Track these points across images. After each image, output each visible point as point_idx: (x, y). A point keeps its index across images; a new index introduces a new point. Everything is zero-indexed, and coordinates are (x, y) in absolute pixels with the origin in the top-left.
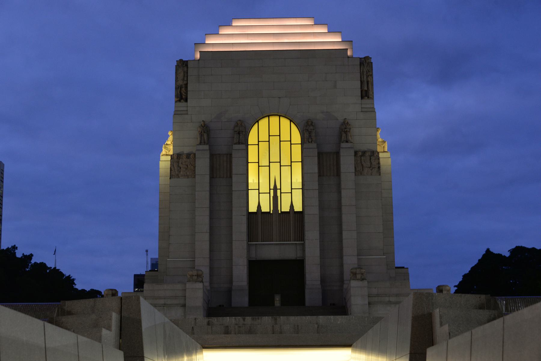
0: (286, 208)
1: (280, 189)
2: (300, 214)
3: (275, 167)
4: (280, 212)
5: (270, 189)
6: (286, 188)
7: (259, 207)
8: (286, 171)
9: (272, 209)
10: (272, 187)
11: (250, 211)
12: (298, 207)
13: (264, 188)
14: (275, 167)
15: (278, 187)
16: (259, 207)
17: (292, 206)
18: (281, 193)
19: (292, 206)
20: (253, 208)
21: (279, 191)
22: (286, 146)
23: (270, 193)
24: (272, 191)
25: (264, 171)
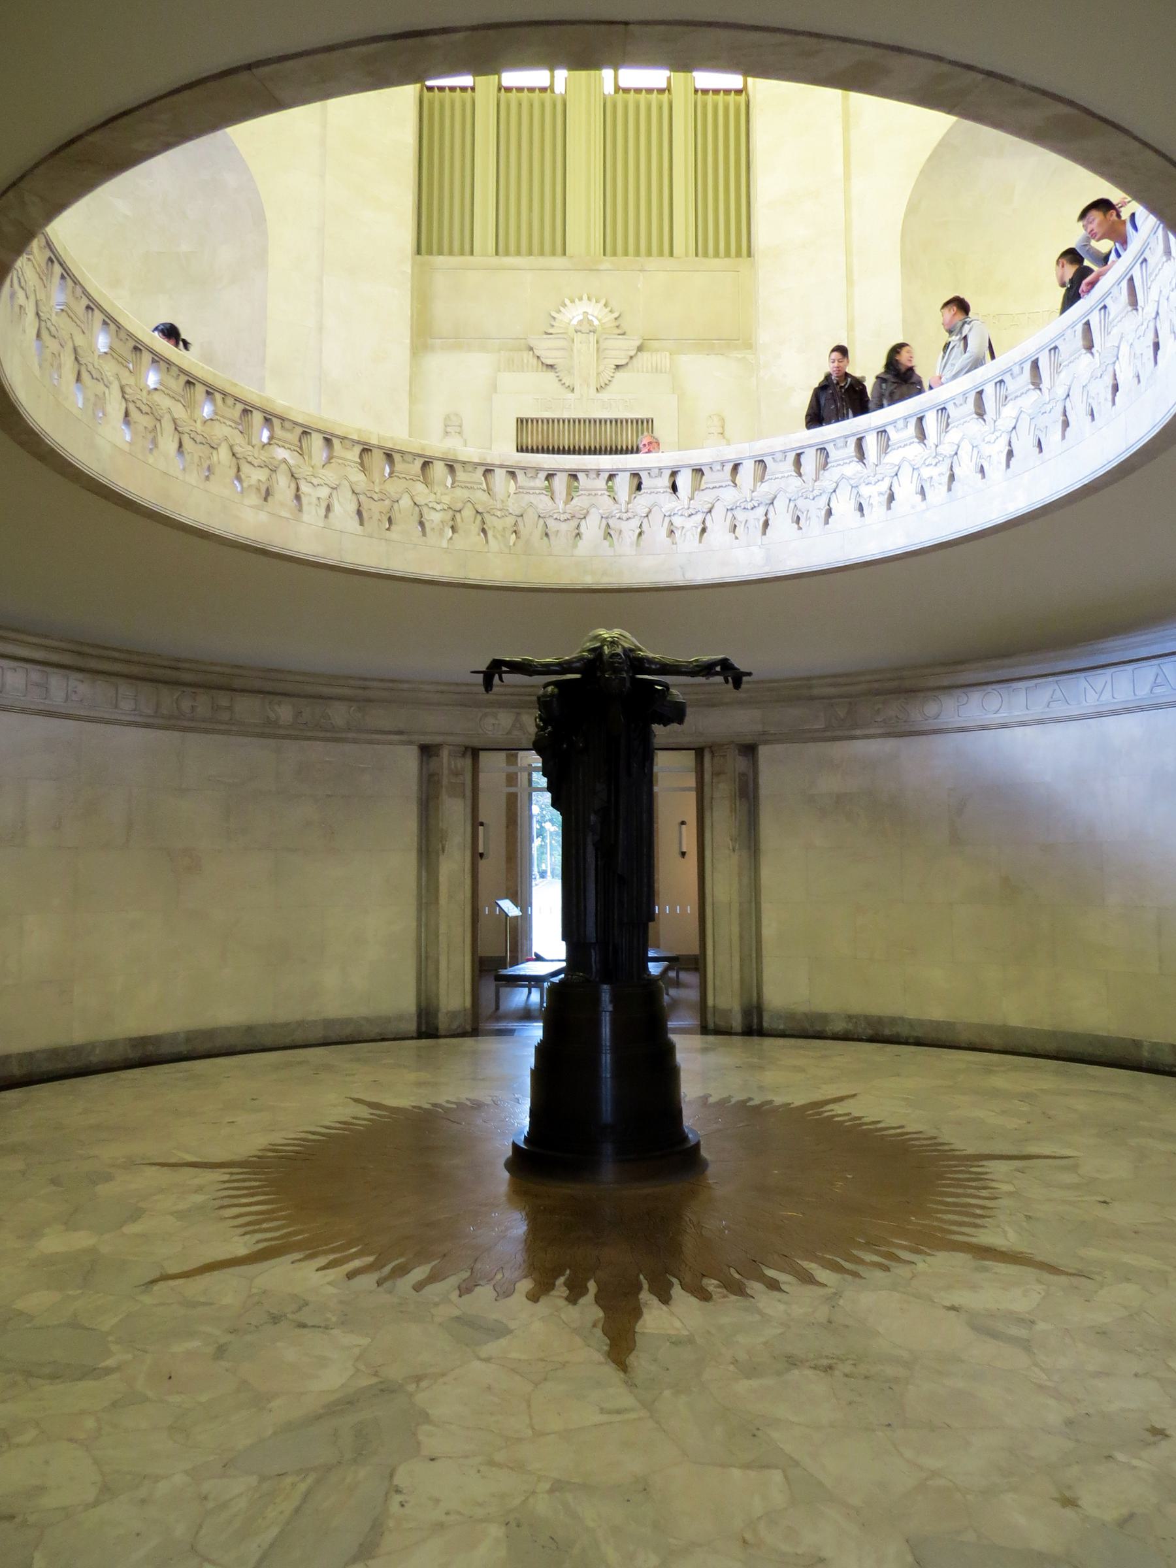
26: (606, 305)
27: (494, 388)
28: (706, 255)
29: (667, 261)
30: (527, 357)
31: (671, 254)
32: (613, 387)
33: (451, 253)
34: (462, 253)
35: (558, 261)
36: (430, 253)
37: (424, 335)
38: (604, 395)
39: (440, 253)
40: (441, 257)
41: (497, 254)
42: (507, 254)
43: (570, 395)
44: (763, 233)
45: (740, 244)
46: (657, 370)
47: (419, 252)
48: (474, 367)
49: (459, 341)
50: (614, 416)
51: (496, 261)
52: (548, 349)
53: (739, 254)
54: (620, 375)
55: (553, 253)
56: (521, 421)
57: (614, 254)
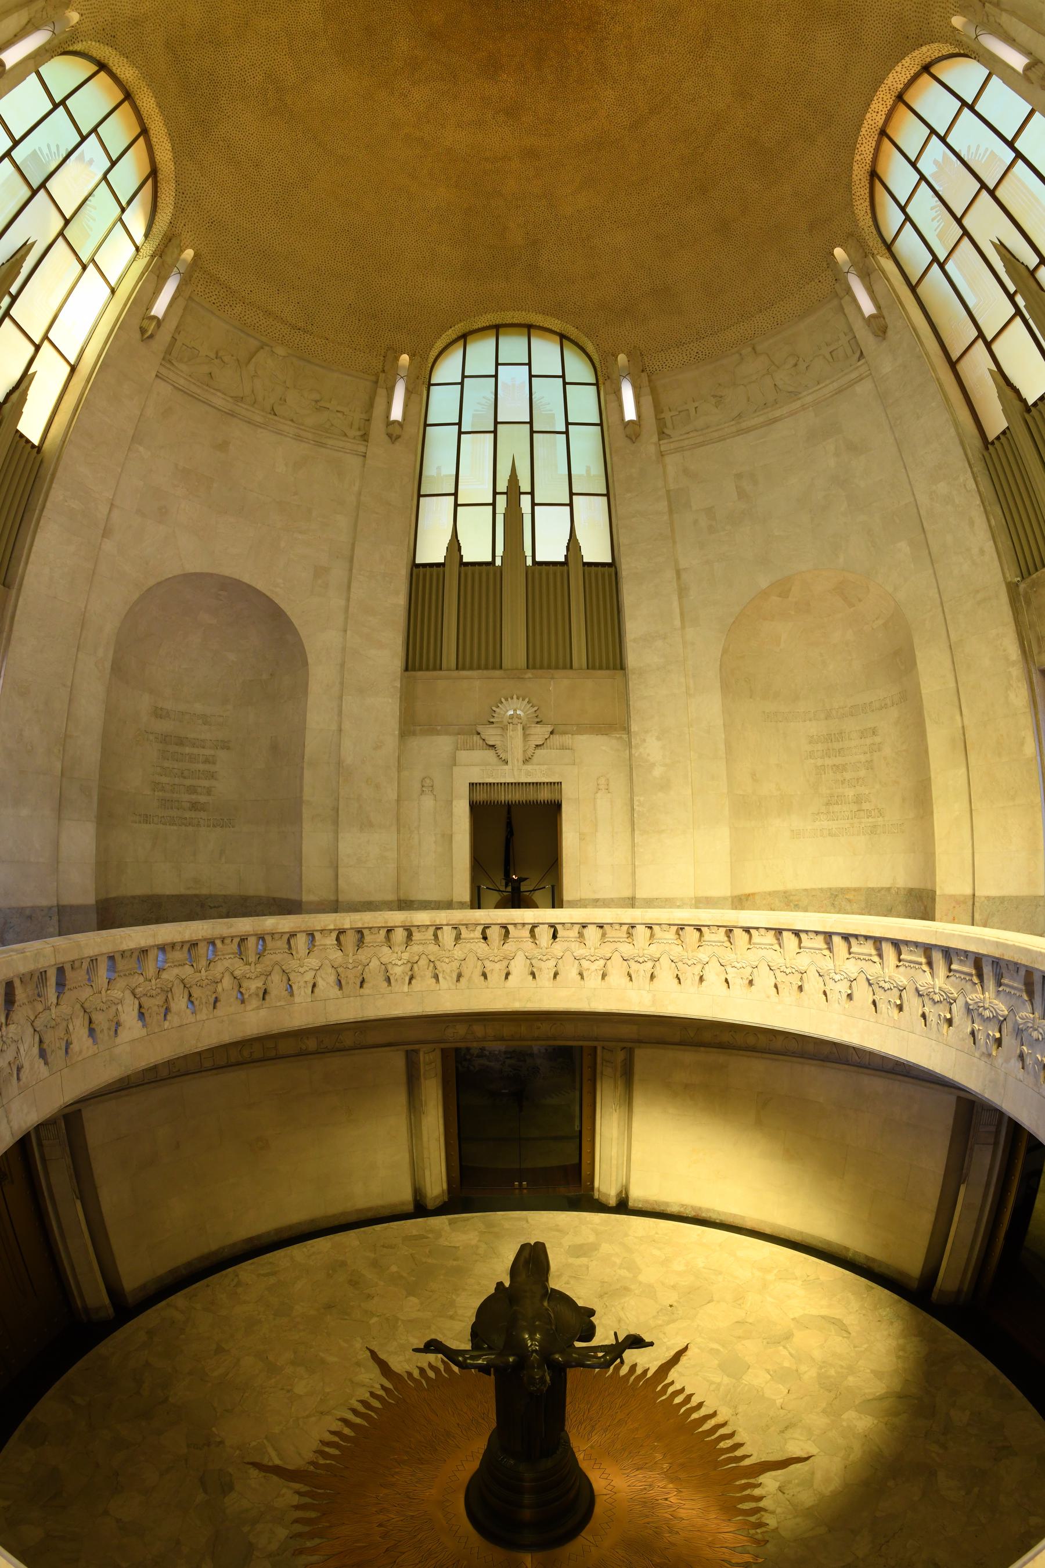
0: (550, 548)
1: (532, 493)
2: (607, 574)
4: (529, 562)
5: (495, 493)
6: (550, 485)
7: (455, 545)
8: (550, 450)
9: (500, 551)
10: (502, 487)
11: (417, 562)
12: (595, 549)
13: (477, 486)
14: (514, 441)
15: (525, 487)
16: (455, 545)
17: (573, 544)
18: (534, 504)
19: (573, 544)
20: (432, 550)
21: (525, 501)
22: (549, 393)
23: (494, 504)
24: (501, 501)
26: (529, 702)
27: (454, 758)
28: (594, 668)
29: (570, 672)
30: (476, 738)
31: (571, 667)
32: (535, 760)
33: (428, 669)
34: (435, 669)
35: (498, 673)
36: (414, 670)
37: (411, 724)
38: (529, 767)
39: (421, 669)
40: (420, 673)
41: (457, 669)
42: (464, 669)
43: (506, 767)
44: (632, 659)
46: (563, 748)
47: (407, 669)
48: (443, 744)
49: (432, 729)
50: (535, 781)
51: (455, 673)
52: (491, 735)
53: (615, 668)
54: (539, 752)
55: (494, 668)
56: (472, 785)
57: (534, 668)
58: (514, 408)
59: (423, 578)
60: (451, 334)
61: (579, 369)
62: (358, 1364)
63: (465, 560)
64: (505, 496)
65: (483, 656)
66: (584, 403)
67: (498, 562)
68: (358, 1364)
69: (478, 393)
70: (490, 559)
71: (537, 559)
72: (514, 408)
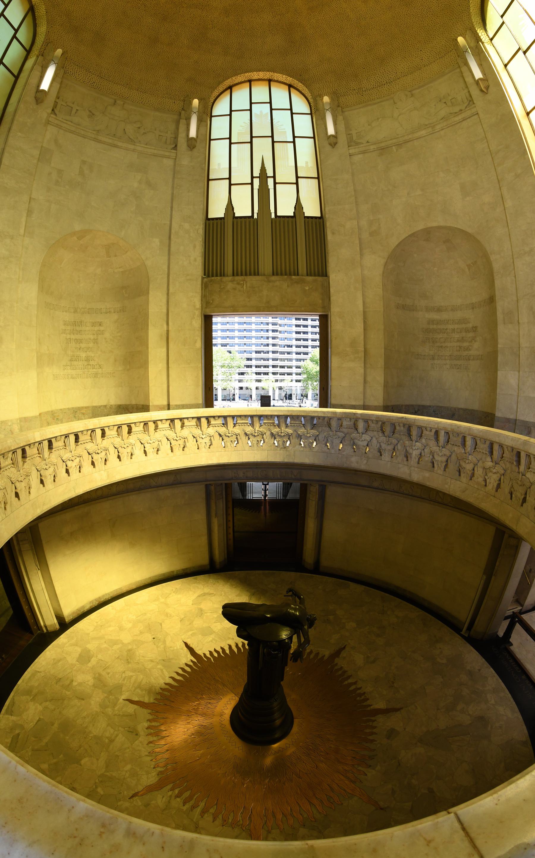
0: (286, 209)
1: (274, 177)
2: (318, 222)
3: (263, 148)
4: (273, 216)
5: (252, 177)
6: (285, 173)
7: (230, 207)
8: (285, 153)
10: (256, 173)
12: (311, 209)
13: (241, 173)
14: (263, 148)
15: (270, 173)
16: (230, 207)
17: (298, 206)
18: (275, 183)
19: (298, 206)
21: (270, 182)
23: (252, 184)
24: (256, 182)
25: (241, 153)
41: (233, 275)
45: (324, 274)
58: (262, 128)
59: (212, 226)
60: (289, 80)
61: (300, 105)
62: (147, 805)
63: (236, 215)
64: (258, 179)
65: (247, 269)
66: (304, 124)
67: (255, 216)
68: (147, 805)
69: (241, 120)
70: (250, 214)
71: (278, 214)
72: (262, 128)
